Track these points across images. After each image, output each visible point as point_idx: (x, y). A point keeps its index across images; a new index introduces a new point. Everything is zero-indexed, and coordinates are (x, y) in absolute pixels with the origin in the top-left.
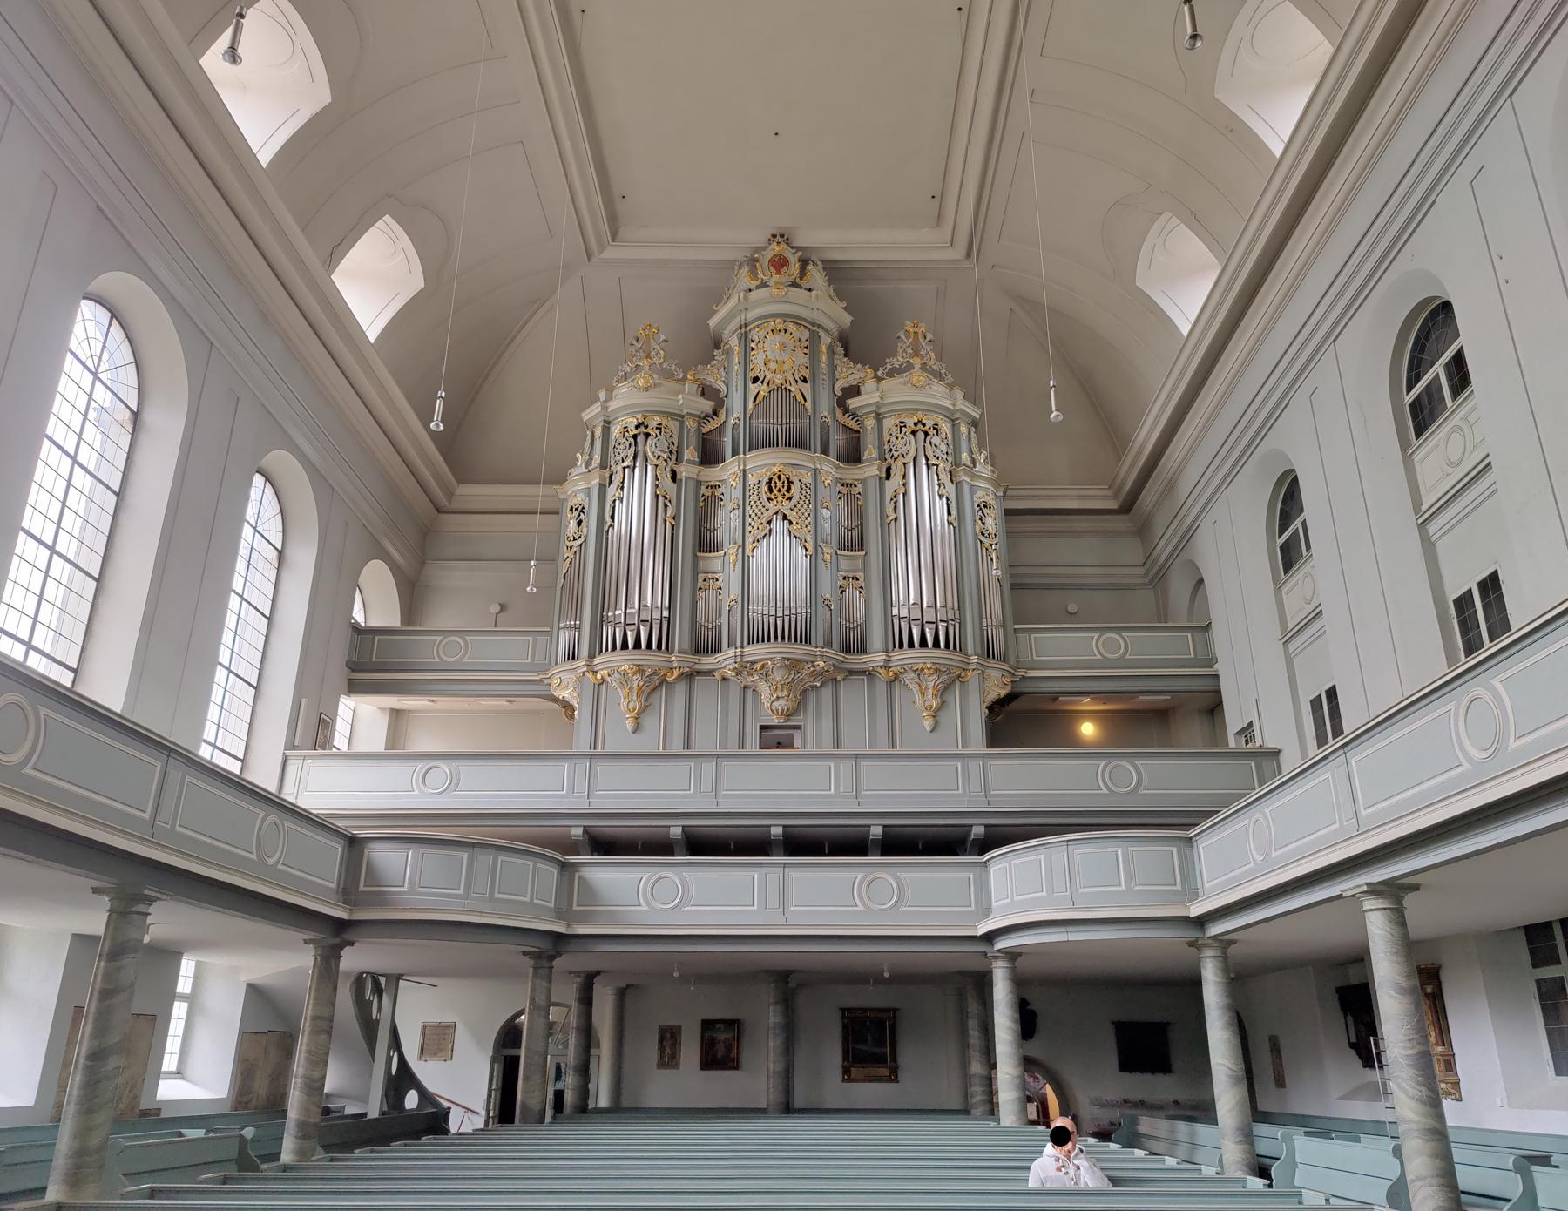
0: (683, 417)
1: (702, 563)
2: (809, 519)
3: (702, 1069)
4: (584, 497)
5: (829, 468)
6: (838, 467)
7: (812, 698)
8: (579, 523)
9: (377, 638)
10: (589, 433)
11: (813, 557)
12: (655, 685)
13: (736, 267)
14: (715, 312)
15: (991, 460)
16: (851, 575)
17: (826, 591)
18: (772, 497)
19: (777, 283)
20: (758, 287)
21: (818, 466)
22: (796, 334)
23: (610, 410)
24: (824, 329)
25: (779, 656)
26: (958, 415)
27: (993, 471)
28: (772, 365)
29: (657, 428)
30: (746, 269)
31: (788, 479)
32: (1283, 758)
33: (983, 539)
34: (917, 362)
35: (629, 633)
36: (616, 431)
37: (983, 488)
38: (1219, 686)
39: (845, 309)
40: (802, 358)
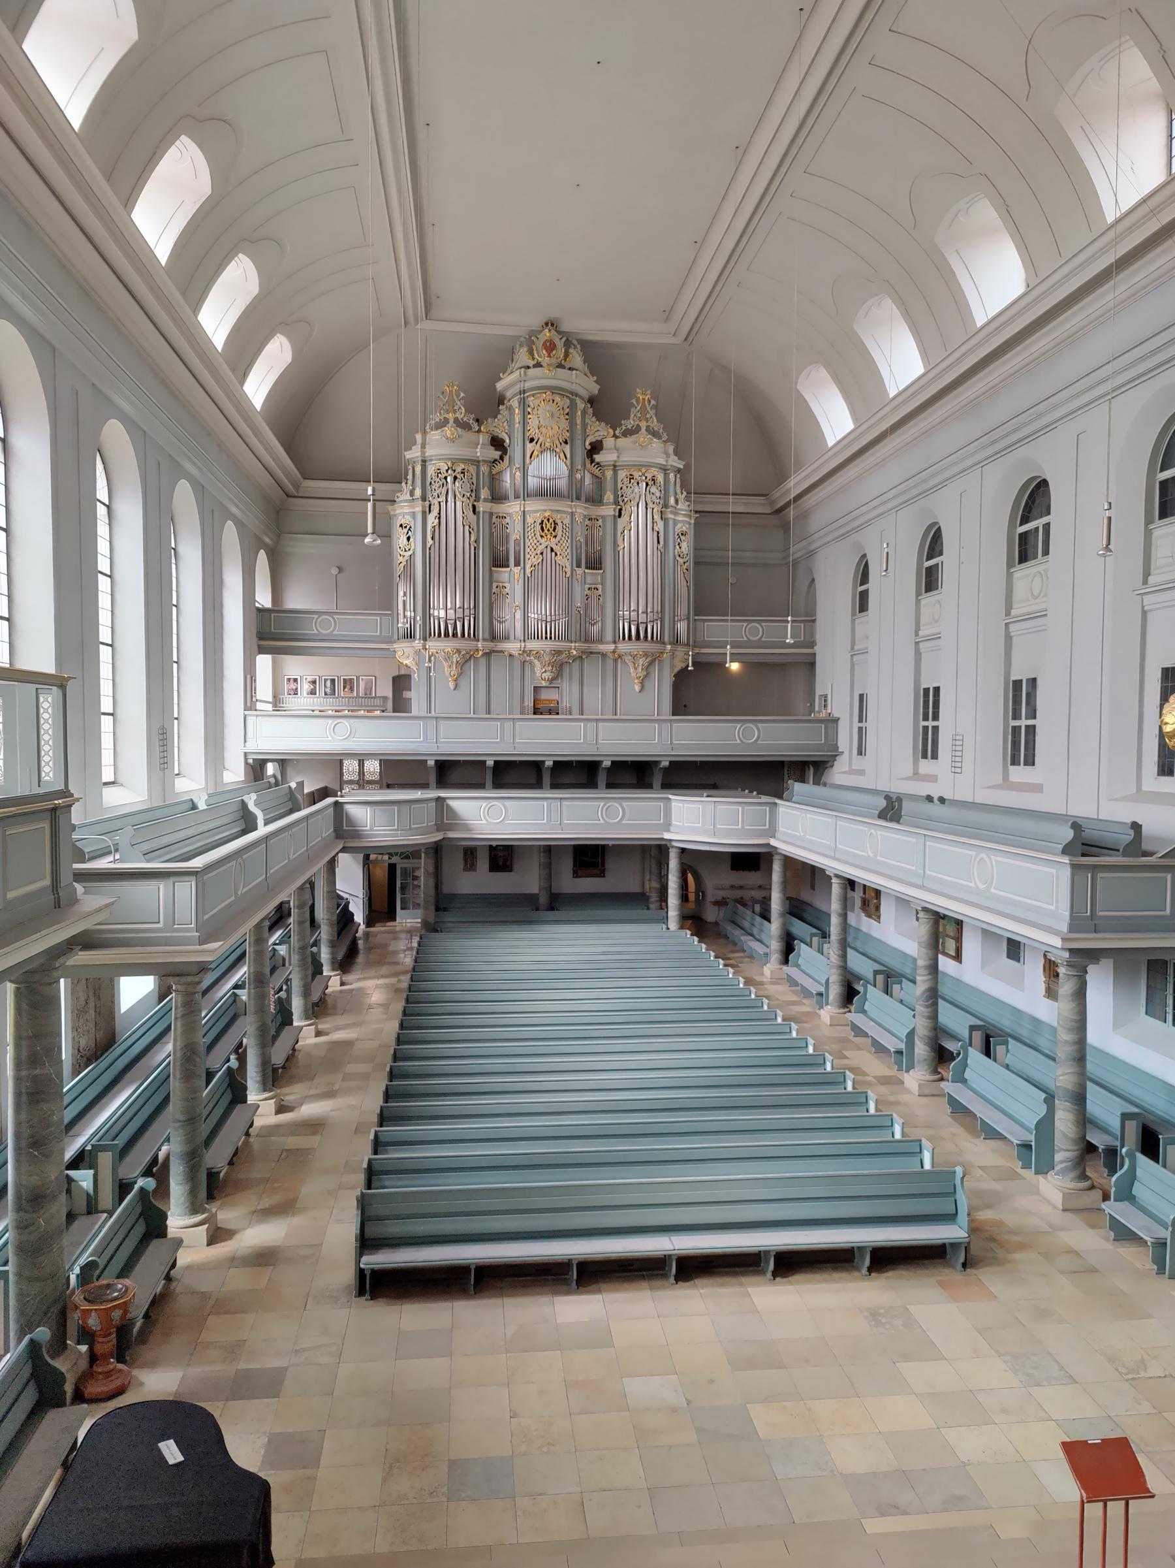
0: (478, 462)
1: (495, 575)
2: (568, 551)
3: (490, 871)
4: (411, 519)
5: (581, 509)
6: (586, 508)
7: (566, 669)
8: (408, 539)
9: (273, 615)
10: (410, 467)
11: (570, 579)
12: (467, 659)
13: (518, 346)
14: (501, 379)
15: (687, 499)
16: (593, 586)
17: (578, 602)
18: (544, 535)
19: (548, 365)
20: (535, 366)
21: (574, 510)
22: (560, 404)
23: (427, 454)
24: (582, 398)
25: (548, 650)
26: (669, 467)
27: (689, 506)
28: (544, 430)
29: (462, 473)
30: (524, 350)
31: (554, 521)
32: (840, 723)
33: (678, 558)
34: (643, 425)
35: (449, 626)
36: (431, 470)
37: (682, 519)
38: (815, 659)
39: (595, 381)
40: (565, 424)
